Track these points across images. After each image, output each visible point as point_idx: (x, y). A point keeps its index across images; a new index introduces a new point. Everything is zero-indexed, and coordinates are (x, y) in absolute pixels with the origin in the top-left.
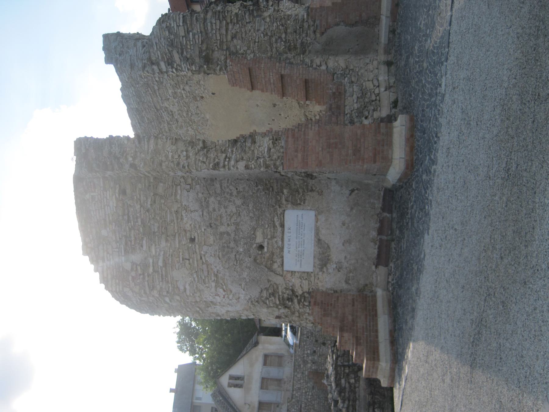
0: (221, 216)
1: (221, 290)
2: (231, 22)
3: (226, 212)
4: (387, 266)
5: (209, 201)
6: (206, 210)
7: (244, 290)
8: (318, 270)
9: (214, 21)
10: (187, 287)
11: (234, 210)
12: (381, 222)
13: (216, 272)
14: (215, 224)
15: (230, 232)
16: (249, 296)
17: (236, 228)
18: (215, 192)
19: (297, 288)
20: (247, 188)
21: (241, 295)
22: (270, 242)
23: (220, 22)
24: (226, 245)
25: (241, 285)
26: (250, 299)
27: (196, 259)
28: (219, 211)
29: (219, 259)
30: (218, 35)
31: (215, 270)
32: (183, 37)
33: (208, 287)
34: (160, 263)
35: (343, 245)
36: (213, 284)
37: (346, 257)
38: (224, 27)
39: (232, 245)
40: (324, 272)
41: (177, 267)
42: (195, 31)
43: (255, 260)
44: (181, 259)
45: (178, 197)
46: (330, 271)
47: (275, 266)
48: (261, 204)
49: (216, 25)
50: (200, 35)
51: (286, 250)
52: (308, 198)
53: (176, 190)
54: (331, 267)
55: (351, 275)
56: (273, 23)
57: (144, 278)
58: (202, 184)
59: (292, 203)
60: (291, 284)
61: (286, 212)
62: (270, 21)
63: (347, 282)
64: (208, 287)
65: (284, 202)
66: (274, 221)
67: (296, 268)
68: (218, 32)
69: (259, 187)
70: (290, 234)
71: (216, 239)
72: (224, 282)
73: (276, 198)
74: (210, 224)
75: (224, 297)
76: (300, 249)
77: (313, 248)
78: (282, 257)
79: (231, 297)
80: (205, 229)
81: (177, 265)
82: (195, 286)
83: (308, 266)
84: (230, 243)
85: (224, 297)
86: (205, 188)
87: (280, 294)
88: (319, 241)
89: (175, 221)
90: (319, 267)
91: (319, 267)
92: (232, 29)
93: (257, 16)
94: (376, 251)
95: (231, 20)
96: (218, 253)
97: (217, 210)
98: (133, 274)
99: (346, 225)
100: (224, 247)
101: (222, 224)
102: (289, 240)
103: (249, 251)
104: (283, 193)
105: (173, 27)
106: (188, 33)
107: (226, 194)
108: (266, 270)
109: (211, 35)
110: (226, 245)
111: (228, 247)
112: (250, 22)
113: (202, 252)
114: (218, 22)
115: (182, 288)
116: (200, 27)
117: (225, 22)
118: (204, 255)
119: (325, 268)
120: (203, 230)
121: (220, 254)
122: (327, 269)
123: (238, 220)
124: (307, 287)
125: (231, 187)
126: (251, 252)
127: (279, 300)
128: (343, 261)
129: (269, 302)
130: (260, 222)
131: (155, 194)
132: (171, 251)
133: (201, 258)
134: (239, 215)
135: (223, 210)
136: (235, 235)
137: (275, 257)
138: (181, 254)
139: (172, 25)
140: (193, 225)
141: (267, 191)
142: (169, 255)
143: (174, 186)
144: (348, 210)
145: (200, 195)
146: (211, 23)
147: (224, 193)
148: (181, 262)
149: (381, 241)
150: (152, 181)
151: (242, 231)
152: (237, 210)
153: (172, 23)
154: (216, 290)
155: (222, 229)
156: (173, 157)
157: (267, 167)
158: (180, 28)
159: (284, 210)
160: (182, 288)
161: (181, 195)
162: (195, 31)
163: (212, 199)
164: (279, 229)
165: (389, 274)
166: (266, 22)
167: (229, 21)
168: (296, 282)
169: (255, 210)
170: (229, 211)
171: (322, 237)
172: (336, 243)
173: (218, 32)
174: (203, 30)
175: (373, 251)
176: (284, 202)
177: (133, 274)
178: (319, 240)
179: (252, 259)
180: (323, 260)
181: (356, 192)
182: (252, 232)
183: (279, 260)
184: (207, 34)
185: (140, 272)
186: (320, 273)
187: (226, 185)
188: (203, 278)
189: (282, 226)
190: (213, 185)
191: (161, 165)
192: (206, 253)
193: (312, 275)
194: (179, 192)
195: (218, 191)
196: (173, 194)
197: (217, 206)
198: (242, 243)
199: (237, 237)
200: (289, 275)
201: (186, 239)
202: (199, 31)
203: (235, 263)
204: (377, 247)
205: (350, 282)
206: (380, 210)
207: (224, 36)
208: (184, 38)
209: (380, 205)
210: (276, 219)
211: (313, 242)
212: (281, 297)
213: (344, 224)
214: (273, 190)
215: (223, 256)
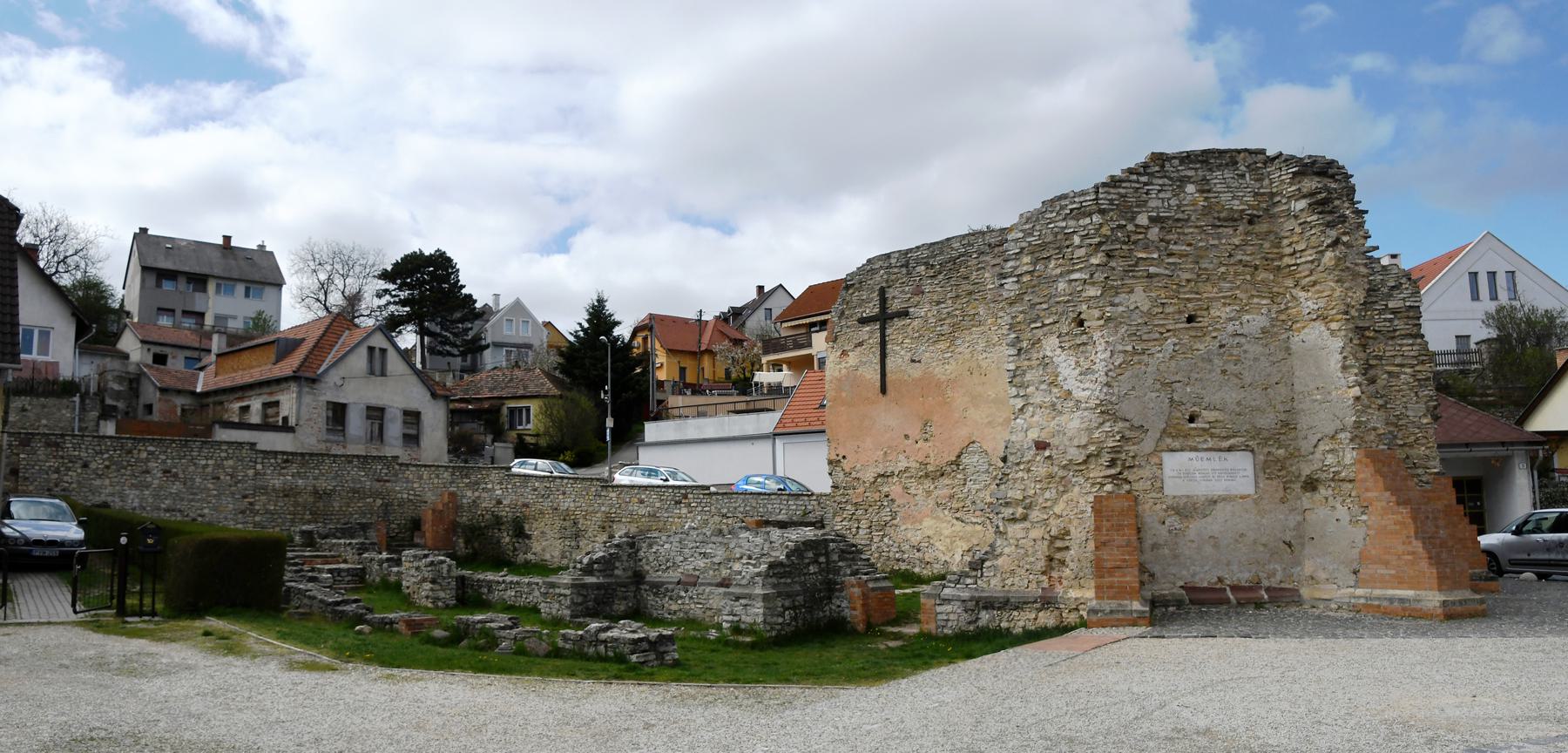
10: (1121, 309)
34: (1152, 270)
36: (1129, 348)
47: (1169, 441)
51: (1193, 455)
52: (1275, 483)
57: (1125, 243)
65: (1266, 450)
83: (1174, 487)
88: (1214, 502)
98: (1130, 227)
131: (1256, 267)
144: (1264, 540)
159: (1252, 451)
160: (1117, 300)
164: (1226, 444)
171: (1220, 506)
172: (1215, 524)
176: (1266, 450)
177: (1130, 227)
183: (1177, 444)
185: (1134, 238)
189: (1230, 449)
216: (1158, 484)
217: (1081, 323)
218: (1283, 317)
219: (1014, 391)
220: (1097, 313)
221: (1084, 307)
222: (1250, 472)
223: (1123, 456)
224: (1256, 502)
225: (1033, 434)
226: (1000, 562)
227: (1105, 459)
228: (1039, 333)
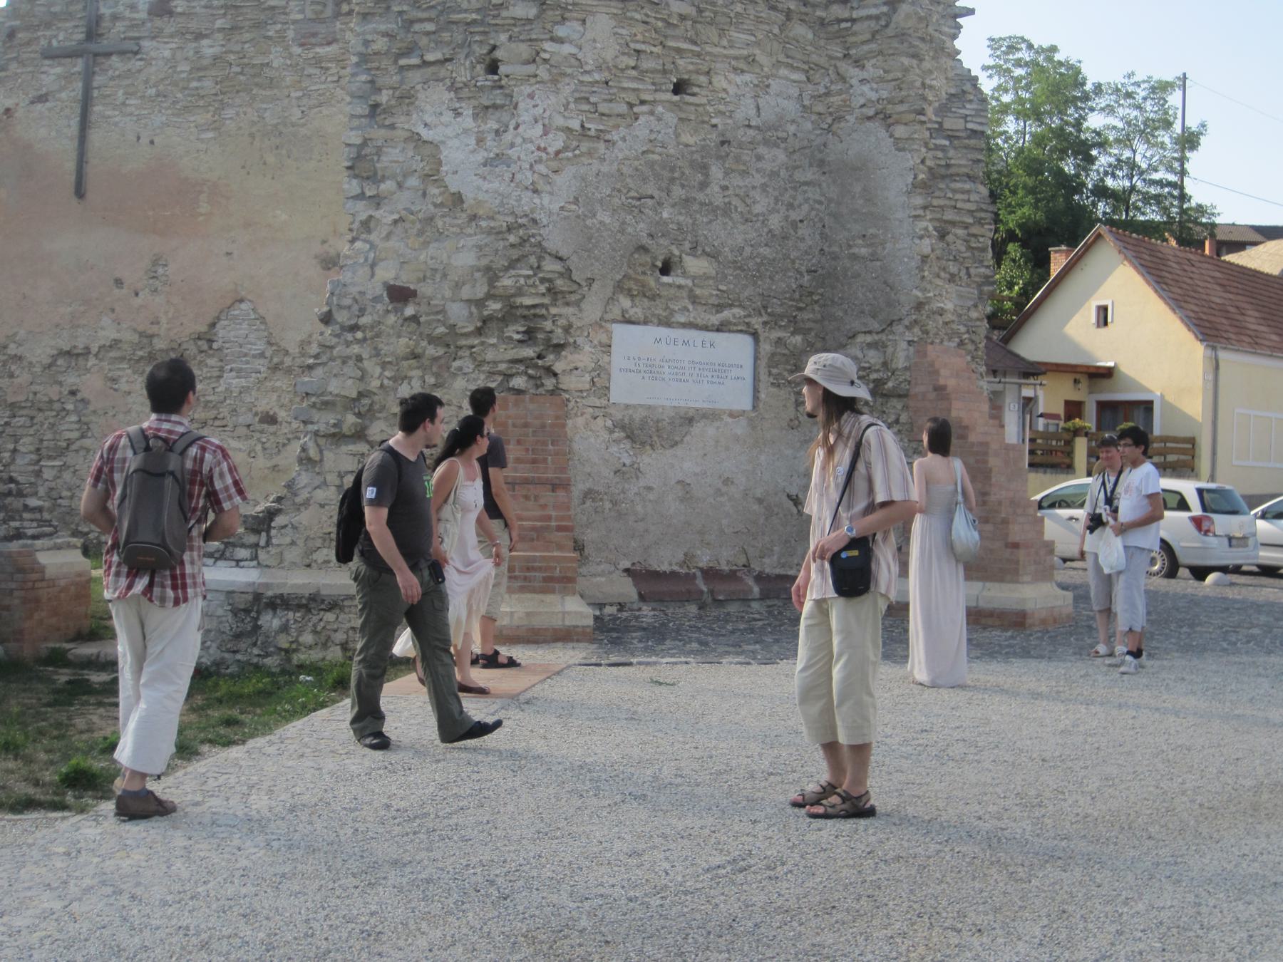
0: (745, 173)
1: (559, 144)
2: (969, 235)
3: (754, 188)
4: (642, 598)
5: (778, 147)
6: (759, 138)
7: (562, 208)
8: (619, 416)
9: (974, 197)
10: (567, 49)
11: (758, 209)
12: (732, 576)
13: (608, 137)
14: (728, 155)
15: (708, 191)
16: (545, 221)
17: (717, 207)
18: (798, 167)
19: (570, 357)
20: (802, 246)
21: (546, 199)
22: (685, 294)
23: (971, 212)
24: (676, 175)
25: (576, 201)
26: (534, 221)
27: (641, 87)
28: (758, 171)
29: (644, 152)
30: (942, 202)
31: (615, 136)
32: (940, 124)
33: (566, 107)
35: (679, 482)
36: (575, 124)
37: (649, 489)
38: (958, 219)
39: (678, 192)
40: (611, 432)
41: (620, 31)
42: (951, 153)
43: (643, 249)
44: (638, 47)
45: (783, 72)
46: (614, 449)
47: (626, 302)
48: (771, 278)
49: (964, 201)
50: (943, 163)
51: (663, 332)
53: (798, 68)
54: (623, 453)
55: (608, 505)
56: (965, 325)
58: (813, 137)
59: (773, 355)
60: (580, 341)
61: (748, 340)
62: (971, 320)
63: (588, 494)
64: (566, 107)
66: (731, 306)
67: (617, 360)
68: (947, 202)
69: (807, 278)
70: (699, 343)
71: (692, 152)
72: (582, 155)
73: (782, 317)
74: (729, 142)
75: (539, 149)
76: (666, 370)
77: (668, 403)
78: (645, 323)
79: (541, 168)
80: (715, 126)
81: (624, 32)
82: (569, 71)
83: (628, 390)
84: (683, 186)
85: (539, 149)
86: (805, 143)
87: (553, 311)
88: (689, 419)
89: (731, 52)
90: (626, 421)
91: (626, 421)
92: (956, 235)
93: (981, 293)
94: (665, 567)
95: (975, 236)
96: (658, 150)
97: (760, 165)
99: (724, 489)
100: (672, 170)
101: (726, 174)
102: (686, 343)
103: (663, 235)
104: (793, 334)
105: (964, 107)
106: (949, 137)
107: (791, 192)
108: (618, 277)
109: (942, 186)
110: (676, 175)
111: (672, 180)
112: (969, 275)
113: (660, 109)
114: (972, 207)
115: (561, 31)
116: (960, 166)
117: (971, 221)
118: (652, 113)
119: (623, 435)
120: (714, 121)
121: (656, 157)
122: (617, 441)
123: (735, 216)
124: (572, 386)
125: (806, 207)
126: (661, 241)
127: (534, 306)
128: (642, 483)
129: (528, 277)
130: (730, 271)
132: (660, 24)
133: (643, 102)
134: (747, 220)
135: (759, 180)
136: (702, 204)
137: (646, 302)
138: (655, 50)
139: (968, 106)
140: (724, 96)
141: (797, 295)
142: (647, 15)
143: (806, 67)
144: (759, 492)
145: (792, 129)
146: (968, 192)
147: (795, 189)
148: (632, 45)
149: (690, 578)
150: (819, 13)
151: (710, 222)
152: (757, 215)
153: (974, 106)
154: (558, 129)
155: (716, 172)
156: (931, 87)
157: (919, 306)
158: (962, 121)
159: (755, 335)
160: (561, 31)
161: (787, 79)
162: (951, 153)
163: (782, 157)
164: (715, 319)
165: (621, 607)
166: (969, 309)
167: (974, 230)
168: (584, 357)
169: (758, 260)
170: (756, 194)
171: (697, 428)
173: (947, 202)
174: (952, 171)
175: (665, 560)
178: (690, 421)
179: (646, 241)
180: (640, 431)
181: (794, 510)
182: (708, 249)
184: (943, 177)
186: (609, 423)
187: (810, 195)
188: (593, 99)
190: (811, 165)
191: (914, 56)
192: (659, 119)
193: (604, 402)
194: (795, 76)
195: (799, 176)
196: (790, 61)
197: (767, 166)
198: (681, 218)
199: (696, 207)
200: (604, 338)
201: (690, 72)
202: (953, 162)
203: (633, 194)
204: (676, 568)
205: (589, 503)
206: (758, 569)
207: (939, 216)
208: (936, 126)
209: (767, 570)
210: (737, 311)
211: (682, 404)
212: (544, 311)
213: (727, 481)
214: (800, 309)
215: (651, 165)
216: (600, 384)
217: (493, 68)
218: (820, 108)
219: (354, 187)
220: (524, 50)
221: (503, 37)
222: (747, 373)
223: (548, 325)
224: (752, 423)
225: (387, 273)
226: (304, 517)
227: (514, 331)
228: (415, 77)
